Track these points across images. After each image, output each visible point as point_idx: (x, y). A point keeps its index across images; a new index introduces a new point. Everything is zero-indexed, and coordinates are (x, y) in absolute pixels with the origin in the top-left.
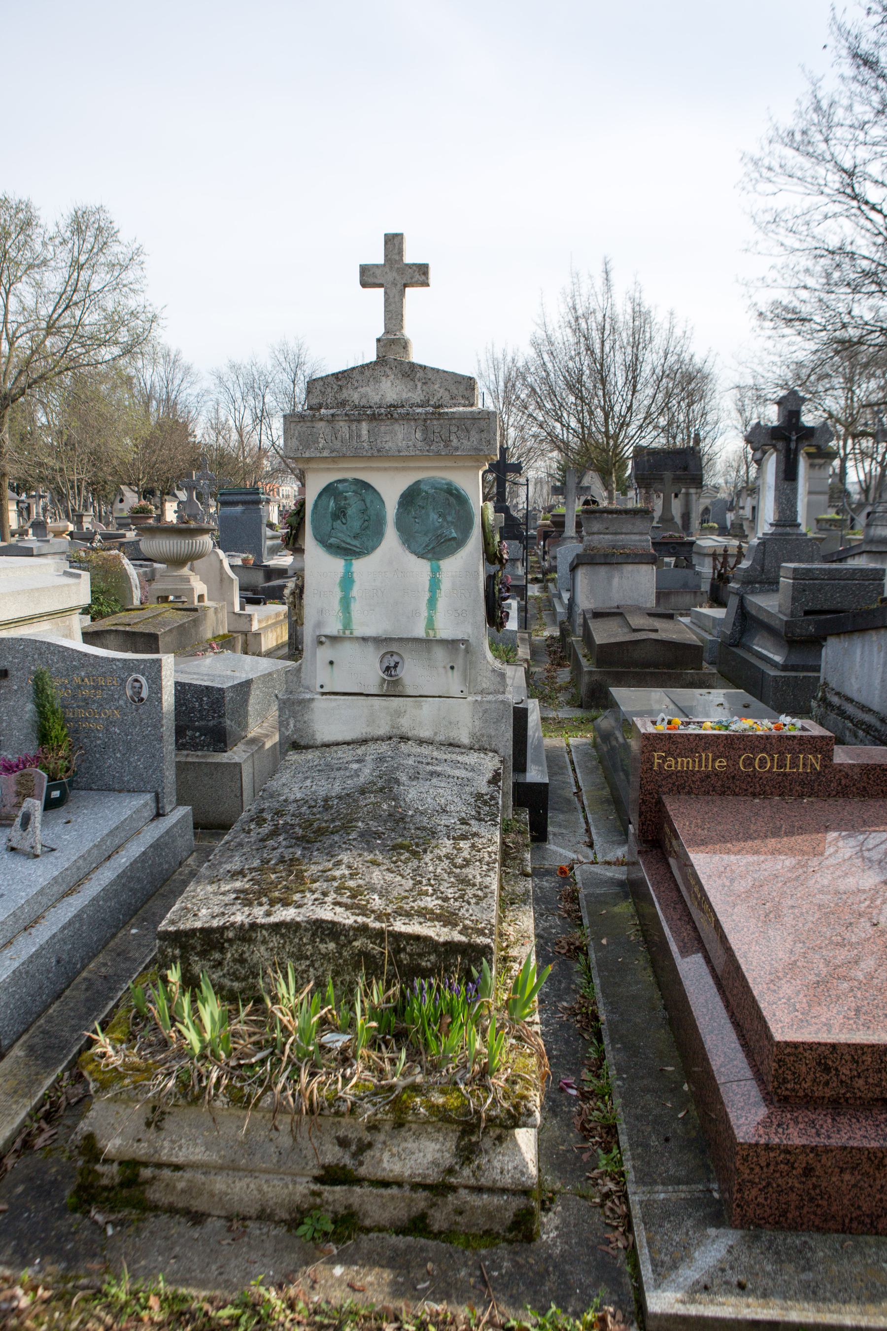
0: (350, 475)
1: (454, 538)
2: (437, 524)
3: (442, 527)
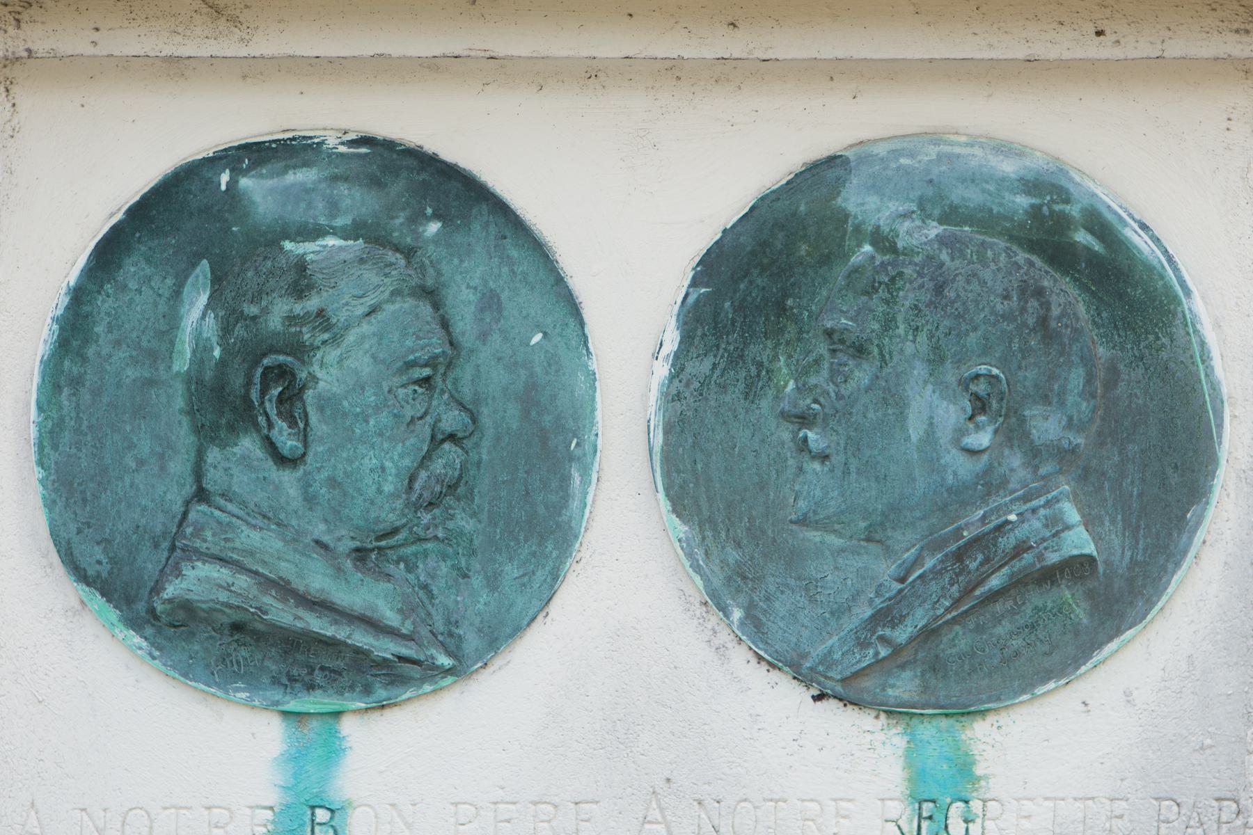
0: (333, 114)
1: (1079, 567)
2: (961, 467)
3: (990, 483)
